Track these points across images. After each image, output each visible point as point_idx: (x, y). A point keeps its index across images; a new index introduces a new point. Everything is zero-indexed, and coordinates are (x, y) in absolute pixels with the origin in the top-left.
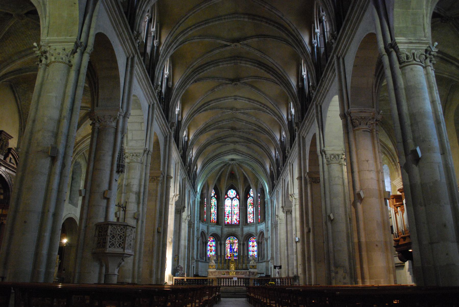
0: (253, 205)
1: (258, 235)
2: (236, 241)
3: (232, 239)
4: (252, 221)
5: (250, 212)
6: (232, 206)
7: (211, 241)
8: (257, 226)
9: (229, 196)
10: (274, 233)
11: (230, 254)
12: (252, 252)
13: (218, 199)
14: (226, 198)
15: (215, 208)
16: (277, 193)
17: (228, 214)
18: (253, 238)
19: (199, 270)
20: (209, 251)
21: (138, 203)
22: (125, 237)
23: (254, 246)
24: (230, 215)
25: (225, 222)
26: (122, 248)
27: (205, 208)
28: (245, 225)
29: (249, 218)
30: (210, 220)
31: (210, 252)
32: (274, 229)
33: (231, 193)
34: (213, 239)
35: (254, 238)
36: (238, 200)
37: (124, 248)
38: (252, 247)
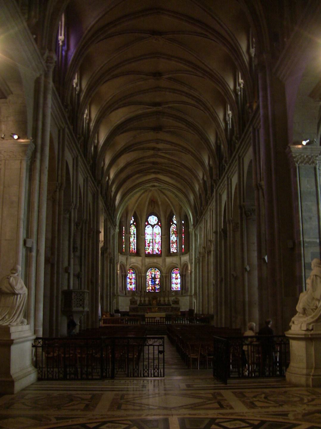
0: (176, 233)
3: (153, 270)
4: (176, 251)
5: (173, 240)
6: (154, 235)
7: (130, 273)
9: (150, 222)
10: (198, 268)
11: (152, 287)
12: (176, 284)
13: (137, 227)
14: (146, 226)
15: (135, 237)
16: (200, 229)
17: (149, 242)
18: (176, 269)
19: (120, 304)
20: (129, 284)
21: (81, 266)
22: (84, 300)
23: (177, 278)
24: (151, 244)
25: (146, 253)
26: (82, 307)
27: (124, 237)
28: (168, 256)
29: (172, 247)
30: (130, 250)
31: (130, 285)
32: (198, 264)
34: (133, 271)
35: (177, 269)
37: (84, 308)
38: (176, 279)
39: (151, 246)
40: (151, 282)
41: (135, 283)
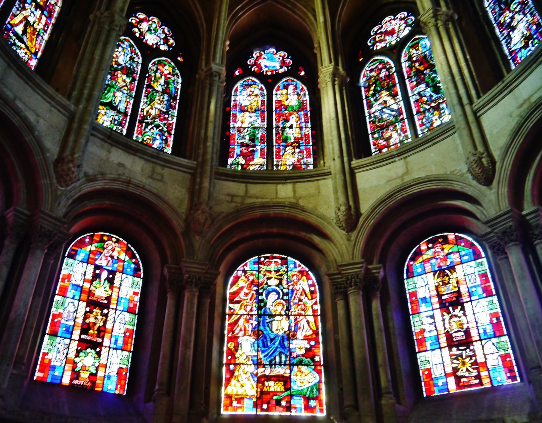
2: (304, 284)
3: (273, 267)
5: (385, 116)
8: (478, 120)
11: (261, 380)
12: (451, 343)
15: (170, 107)
17: (247, 141)
18: (434, 242)
31: (84, 345)
33: (263, 62)
35: (446, 241)
36: (300, 85)
38: (444, 306)
39: (257, 155)
40: (252, 339)
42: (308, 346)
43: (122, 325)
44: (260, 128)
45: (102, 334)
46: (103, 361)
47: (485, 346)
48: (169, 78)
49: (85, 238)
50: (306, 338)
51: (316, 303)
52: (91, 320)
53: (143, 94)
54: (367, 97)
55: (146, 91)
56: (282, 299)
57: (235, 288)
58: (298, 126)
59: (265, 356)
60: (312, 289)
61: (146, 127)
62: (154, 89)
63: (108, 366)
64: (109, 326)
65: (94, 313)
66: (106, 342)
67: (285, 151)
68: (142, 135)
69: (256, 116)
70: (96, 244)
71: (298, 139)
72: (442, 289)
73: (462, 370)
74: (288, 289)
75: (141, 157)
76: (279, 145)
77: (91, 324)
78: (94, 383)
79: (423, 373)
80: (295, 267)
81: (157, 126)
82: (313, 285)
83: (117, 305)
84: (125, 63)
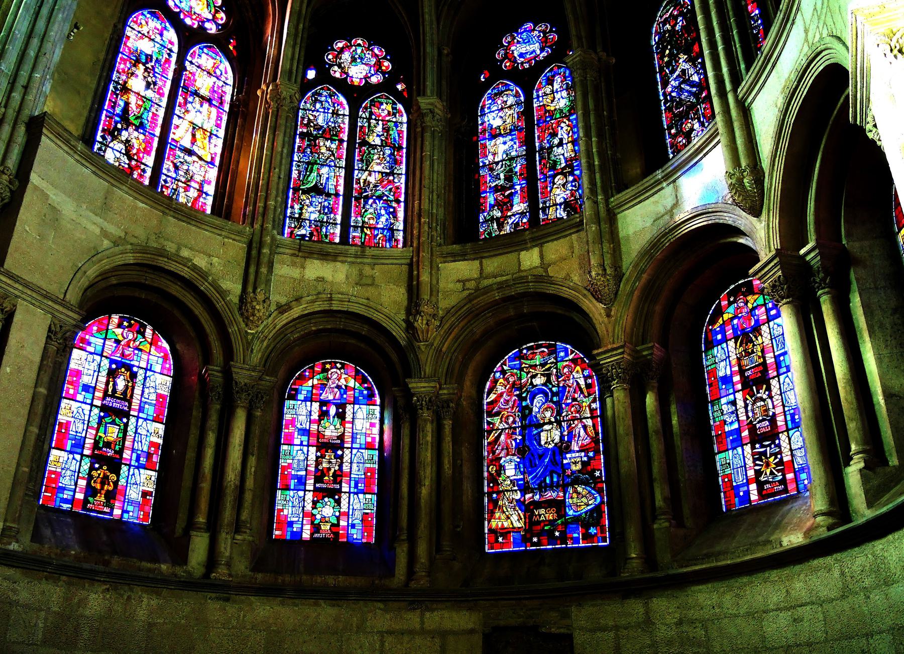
1: (774, 183)
3: (538, 360)
18: (735, 293)
20: (310, 482)
31: (322, 494)
33: (517, 50)
38: (748, 385)
39: (516, 199)
41: (367, 481)
42: (585, 459)
43: (361, 465)
44: (518, 156)
45: (339, 479)
46: (344, 508)
47: (793, 439)
48: (389, 121)
49: (305, 371)
50: (583, 449)
51: (594, 401)
52: (325, 465)
53: (357, 158)
54: (661, 68)
55: (360, 151)
56: (552, 401)
57: (493, 397)
58: (570, 139)
59: (532, 479)
60: (590, 381)
61: (366, 203)
62: (371, 146)
63: (351, 513)
64: (346, 468)
65: (327, 457)
66: (345, 488)
67: (554, 184)
68: (362, 216)
69: (512, 140)
70: (318, 377)
71: (571, 159)
72: (745, 362)
73: (766, 474)
74: (558, 386)
75: (342, 262)
76: (545, 175)
77: (325, 471)
78: (337, 534)
79: (723, 481)
80: (567, 355)
81: (380, 198)
82: (590, 377)
83: (352, 442)
84: (327, 123)
